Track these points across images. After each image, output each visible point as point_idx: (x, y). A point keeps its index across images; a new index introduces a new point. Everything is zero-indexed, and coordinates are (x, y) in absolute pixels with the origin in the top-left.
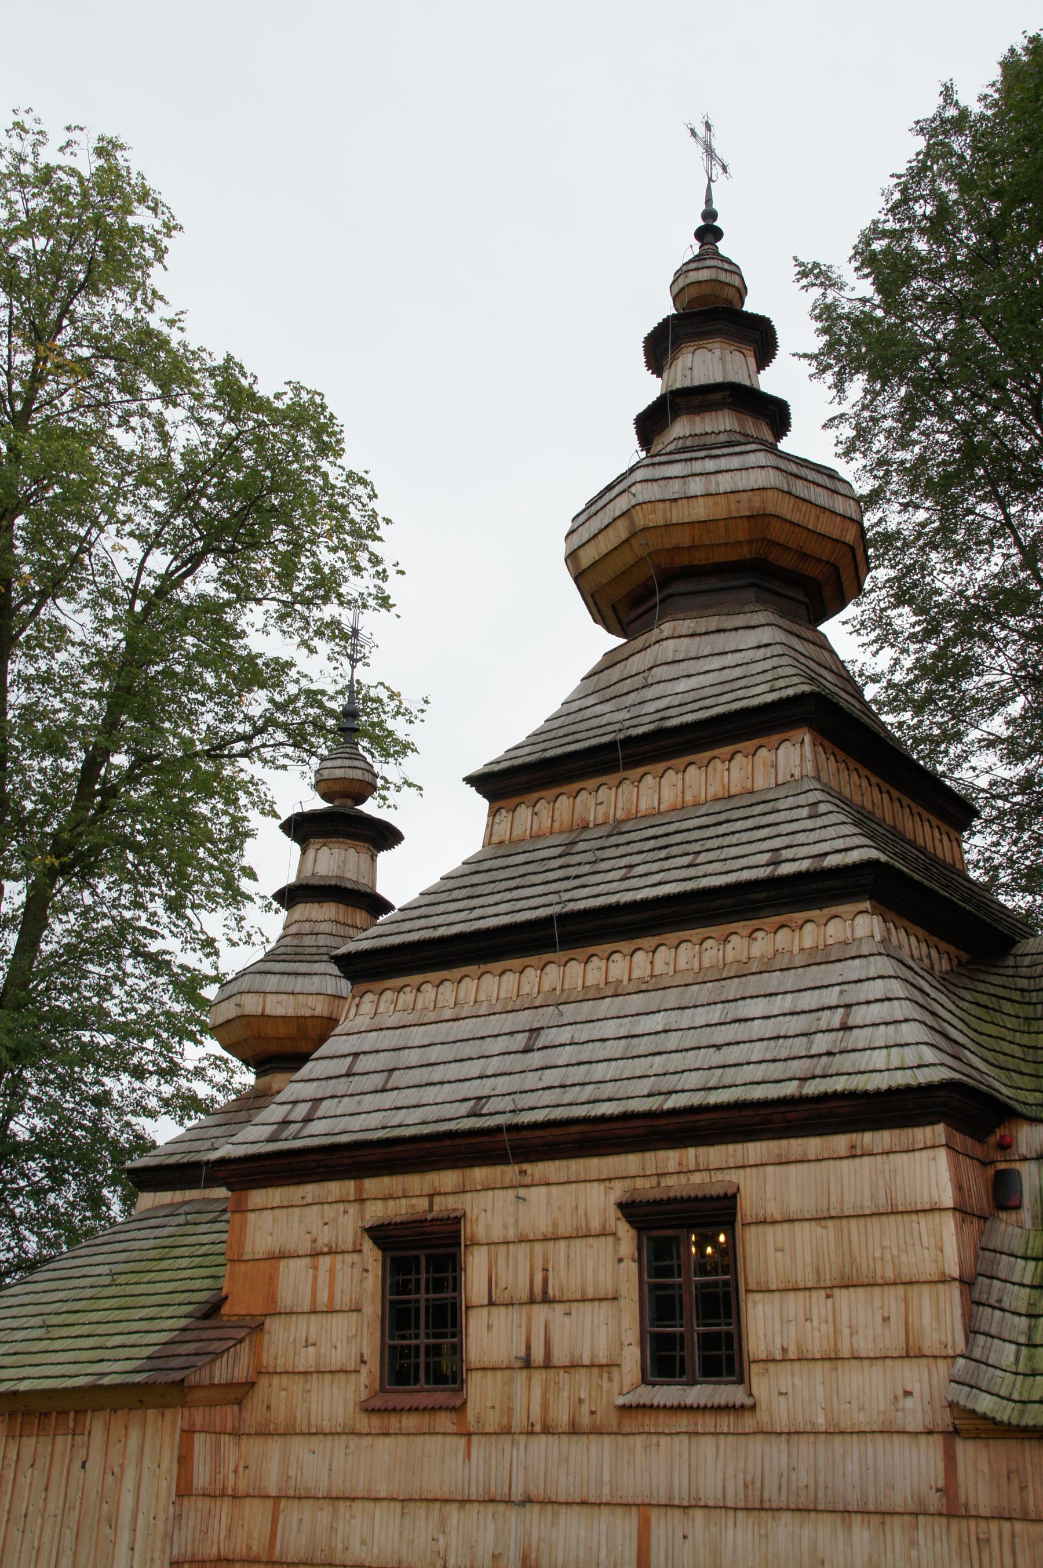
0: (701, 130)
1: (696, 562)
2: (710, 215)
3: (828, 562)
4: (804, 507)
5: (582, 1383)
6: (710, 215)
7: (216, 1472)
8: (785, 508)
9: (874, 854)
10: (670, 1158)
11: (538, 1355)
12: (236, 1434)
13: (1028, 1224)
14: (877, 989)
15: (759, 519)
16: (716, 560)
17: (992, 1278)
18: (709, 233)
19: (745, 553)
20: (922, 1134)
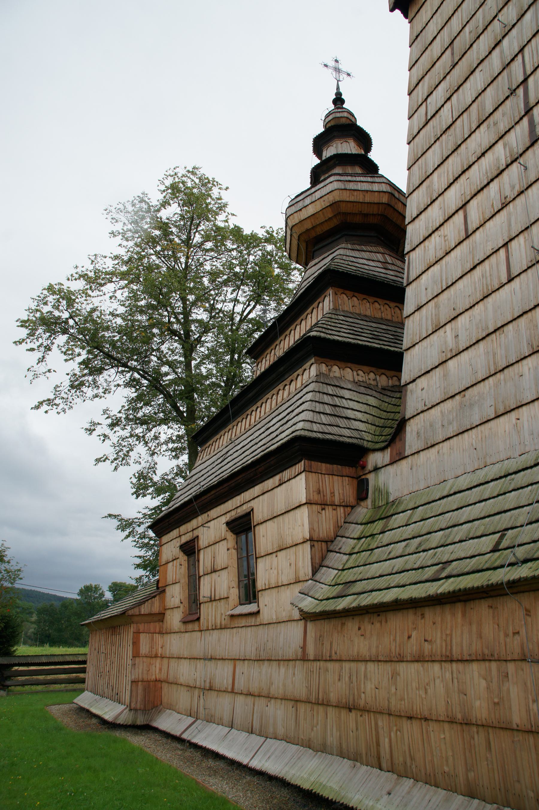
0: (332, 64)
1: (319, 233)
3: (379, 215)
4: (355, 193)
7: (152, 648)
8: (346, 196)
12: (160, 633)
13: (370, 507)
15: (334, 205)
16: (326, 229)
17: (342, 537)
18: (339, 100)
19: (335, 222)
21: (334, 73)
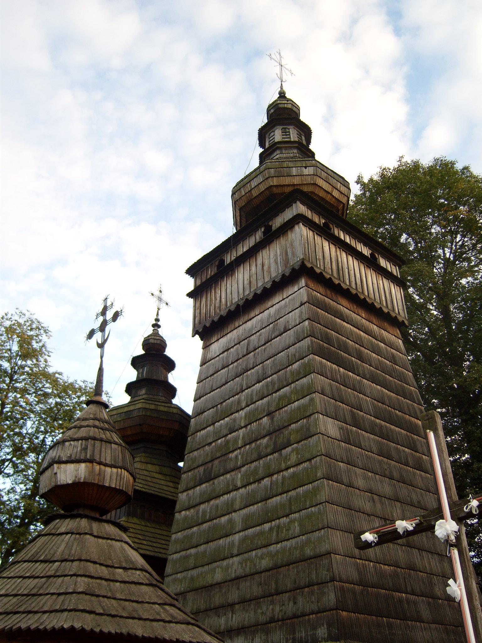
0: (157, 293)
2: (157, 320)
6: (157, 320)
18: (156, 326)
21: (157, 301)
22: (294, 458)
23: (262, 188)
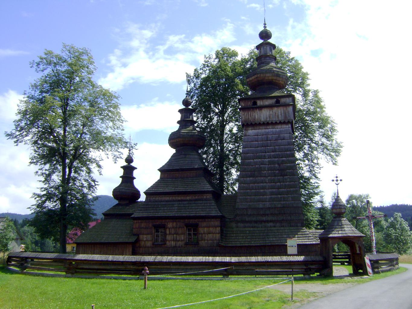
5: (180, 242)
9: (213, 190)
10: (191, 220)
11: (175, 240)
14: (213, 204)
20: (218, 220)
22: (288, 180)
23: (270, 78)
